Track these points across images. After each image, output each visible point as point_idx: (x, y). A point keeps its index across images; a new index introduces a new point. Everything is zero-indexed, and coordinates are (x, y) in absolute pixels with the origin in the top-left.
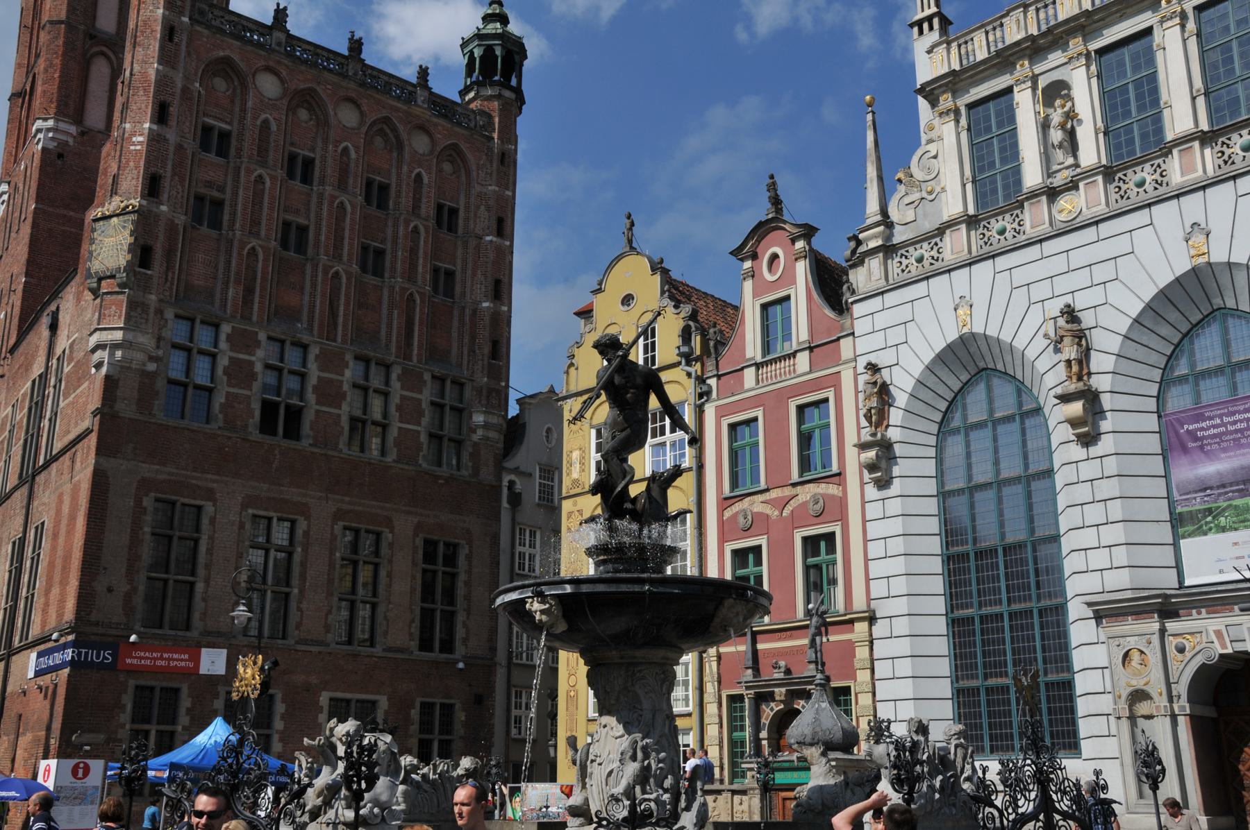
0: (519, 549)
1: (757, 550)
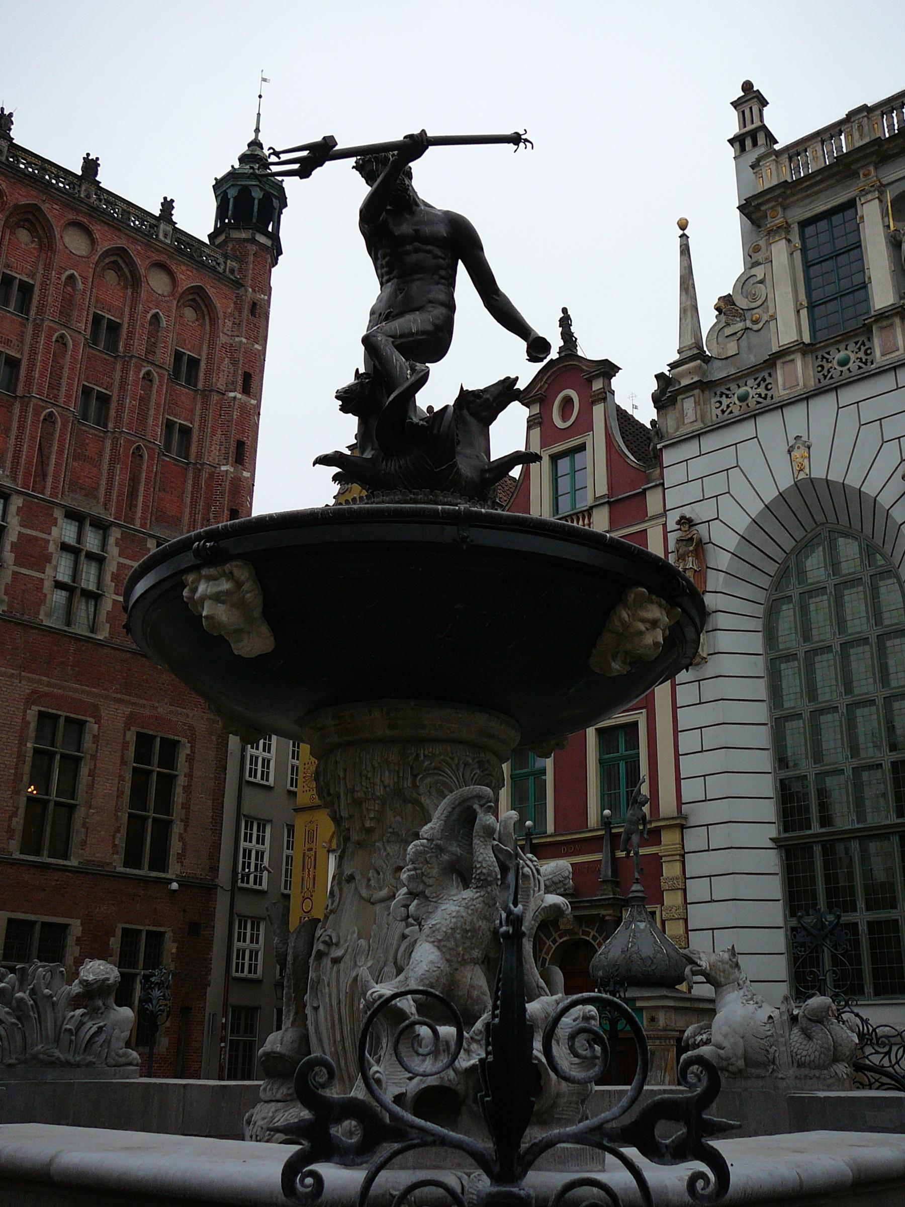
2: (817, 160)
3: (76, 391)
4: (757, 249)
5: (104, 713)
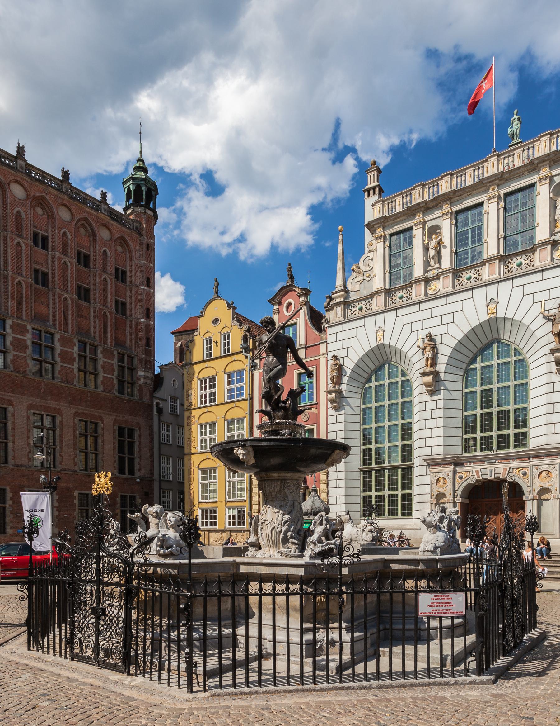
3: (75, 287)
5: (104, 419)
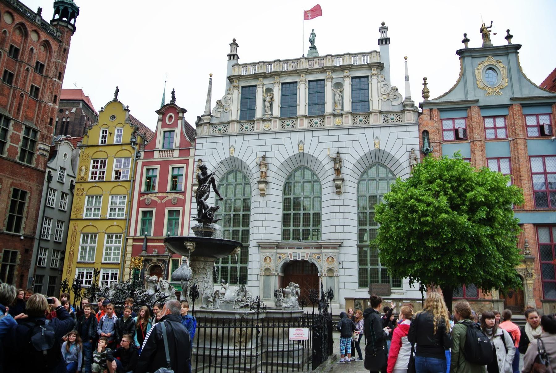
0: (49, 196)
1: (151, 212)
2: (249, 71)
4: (230, 90)
